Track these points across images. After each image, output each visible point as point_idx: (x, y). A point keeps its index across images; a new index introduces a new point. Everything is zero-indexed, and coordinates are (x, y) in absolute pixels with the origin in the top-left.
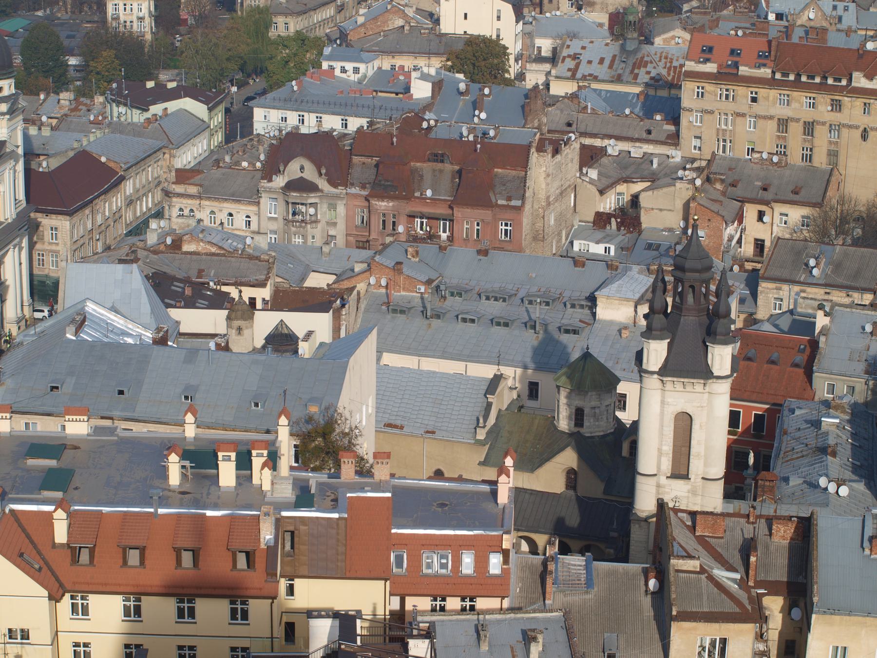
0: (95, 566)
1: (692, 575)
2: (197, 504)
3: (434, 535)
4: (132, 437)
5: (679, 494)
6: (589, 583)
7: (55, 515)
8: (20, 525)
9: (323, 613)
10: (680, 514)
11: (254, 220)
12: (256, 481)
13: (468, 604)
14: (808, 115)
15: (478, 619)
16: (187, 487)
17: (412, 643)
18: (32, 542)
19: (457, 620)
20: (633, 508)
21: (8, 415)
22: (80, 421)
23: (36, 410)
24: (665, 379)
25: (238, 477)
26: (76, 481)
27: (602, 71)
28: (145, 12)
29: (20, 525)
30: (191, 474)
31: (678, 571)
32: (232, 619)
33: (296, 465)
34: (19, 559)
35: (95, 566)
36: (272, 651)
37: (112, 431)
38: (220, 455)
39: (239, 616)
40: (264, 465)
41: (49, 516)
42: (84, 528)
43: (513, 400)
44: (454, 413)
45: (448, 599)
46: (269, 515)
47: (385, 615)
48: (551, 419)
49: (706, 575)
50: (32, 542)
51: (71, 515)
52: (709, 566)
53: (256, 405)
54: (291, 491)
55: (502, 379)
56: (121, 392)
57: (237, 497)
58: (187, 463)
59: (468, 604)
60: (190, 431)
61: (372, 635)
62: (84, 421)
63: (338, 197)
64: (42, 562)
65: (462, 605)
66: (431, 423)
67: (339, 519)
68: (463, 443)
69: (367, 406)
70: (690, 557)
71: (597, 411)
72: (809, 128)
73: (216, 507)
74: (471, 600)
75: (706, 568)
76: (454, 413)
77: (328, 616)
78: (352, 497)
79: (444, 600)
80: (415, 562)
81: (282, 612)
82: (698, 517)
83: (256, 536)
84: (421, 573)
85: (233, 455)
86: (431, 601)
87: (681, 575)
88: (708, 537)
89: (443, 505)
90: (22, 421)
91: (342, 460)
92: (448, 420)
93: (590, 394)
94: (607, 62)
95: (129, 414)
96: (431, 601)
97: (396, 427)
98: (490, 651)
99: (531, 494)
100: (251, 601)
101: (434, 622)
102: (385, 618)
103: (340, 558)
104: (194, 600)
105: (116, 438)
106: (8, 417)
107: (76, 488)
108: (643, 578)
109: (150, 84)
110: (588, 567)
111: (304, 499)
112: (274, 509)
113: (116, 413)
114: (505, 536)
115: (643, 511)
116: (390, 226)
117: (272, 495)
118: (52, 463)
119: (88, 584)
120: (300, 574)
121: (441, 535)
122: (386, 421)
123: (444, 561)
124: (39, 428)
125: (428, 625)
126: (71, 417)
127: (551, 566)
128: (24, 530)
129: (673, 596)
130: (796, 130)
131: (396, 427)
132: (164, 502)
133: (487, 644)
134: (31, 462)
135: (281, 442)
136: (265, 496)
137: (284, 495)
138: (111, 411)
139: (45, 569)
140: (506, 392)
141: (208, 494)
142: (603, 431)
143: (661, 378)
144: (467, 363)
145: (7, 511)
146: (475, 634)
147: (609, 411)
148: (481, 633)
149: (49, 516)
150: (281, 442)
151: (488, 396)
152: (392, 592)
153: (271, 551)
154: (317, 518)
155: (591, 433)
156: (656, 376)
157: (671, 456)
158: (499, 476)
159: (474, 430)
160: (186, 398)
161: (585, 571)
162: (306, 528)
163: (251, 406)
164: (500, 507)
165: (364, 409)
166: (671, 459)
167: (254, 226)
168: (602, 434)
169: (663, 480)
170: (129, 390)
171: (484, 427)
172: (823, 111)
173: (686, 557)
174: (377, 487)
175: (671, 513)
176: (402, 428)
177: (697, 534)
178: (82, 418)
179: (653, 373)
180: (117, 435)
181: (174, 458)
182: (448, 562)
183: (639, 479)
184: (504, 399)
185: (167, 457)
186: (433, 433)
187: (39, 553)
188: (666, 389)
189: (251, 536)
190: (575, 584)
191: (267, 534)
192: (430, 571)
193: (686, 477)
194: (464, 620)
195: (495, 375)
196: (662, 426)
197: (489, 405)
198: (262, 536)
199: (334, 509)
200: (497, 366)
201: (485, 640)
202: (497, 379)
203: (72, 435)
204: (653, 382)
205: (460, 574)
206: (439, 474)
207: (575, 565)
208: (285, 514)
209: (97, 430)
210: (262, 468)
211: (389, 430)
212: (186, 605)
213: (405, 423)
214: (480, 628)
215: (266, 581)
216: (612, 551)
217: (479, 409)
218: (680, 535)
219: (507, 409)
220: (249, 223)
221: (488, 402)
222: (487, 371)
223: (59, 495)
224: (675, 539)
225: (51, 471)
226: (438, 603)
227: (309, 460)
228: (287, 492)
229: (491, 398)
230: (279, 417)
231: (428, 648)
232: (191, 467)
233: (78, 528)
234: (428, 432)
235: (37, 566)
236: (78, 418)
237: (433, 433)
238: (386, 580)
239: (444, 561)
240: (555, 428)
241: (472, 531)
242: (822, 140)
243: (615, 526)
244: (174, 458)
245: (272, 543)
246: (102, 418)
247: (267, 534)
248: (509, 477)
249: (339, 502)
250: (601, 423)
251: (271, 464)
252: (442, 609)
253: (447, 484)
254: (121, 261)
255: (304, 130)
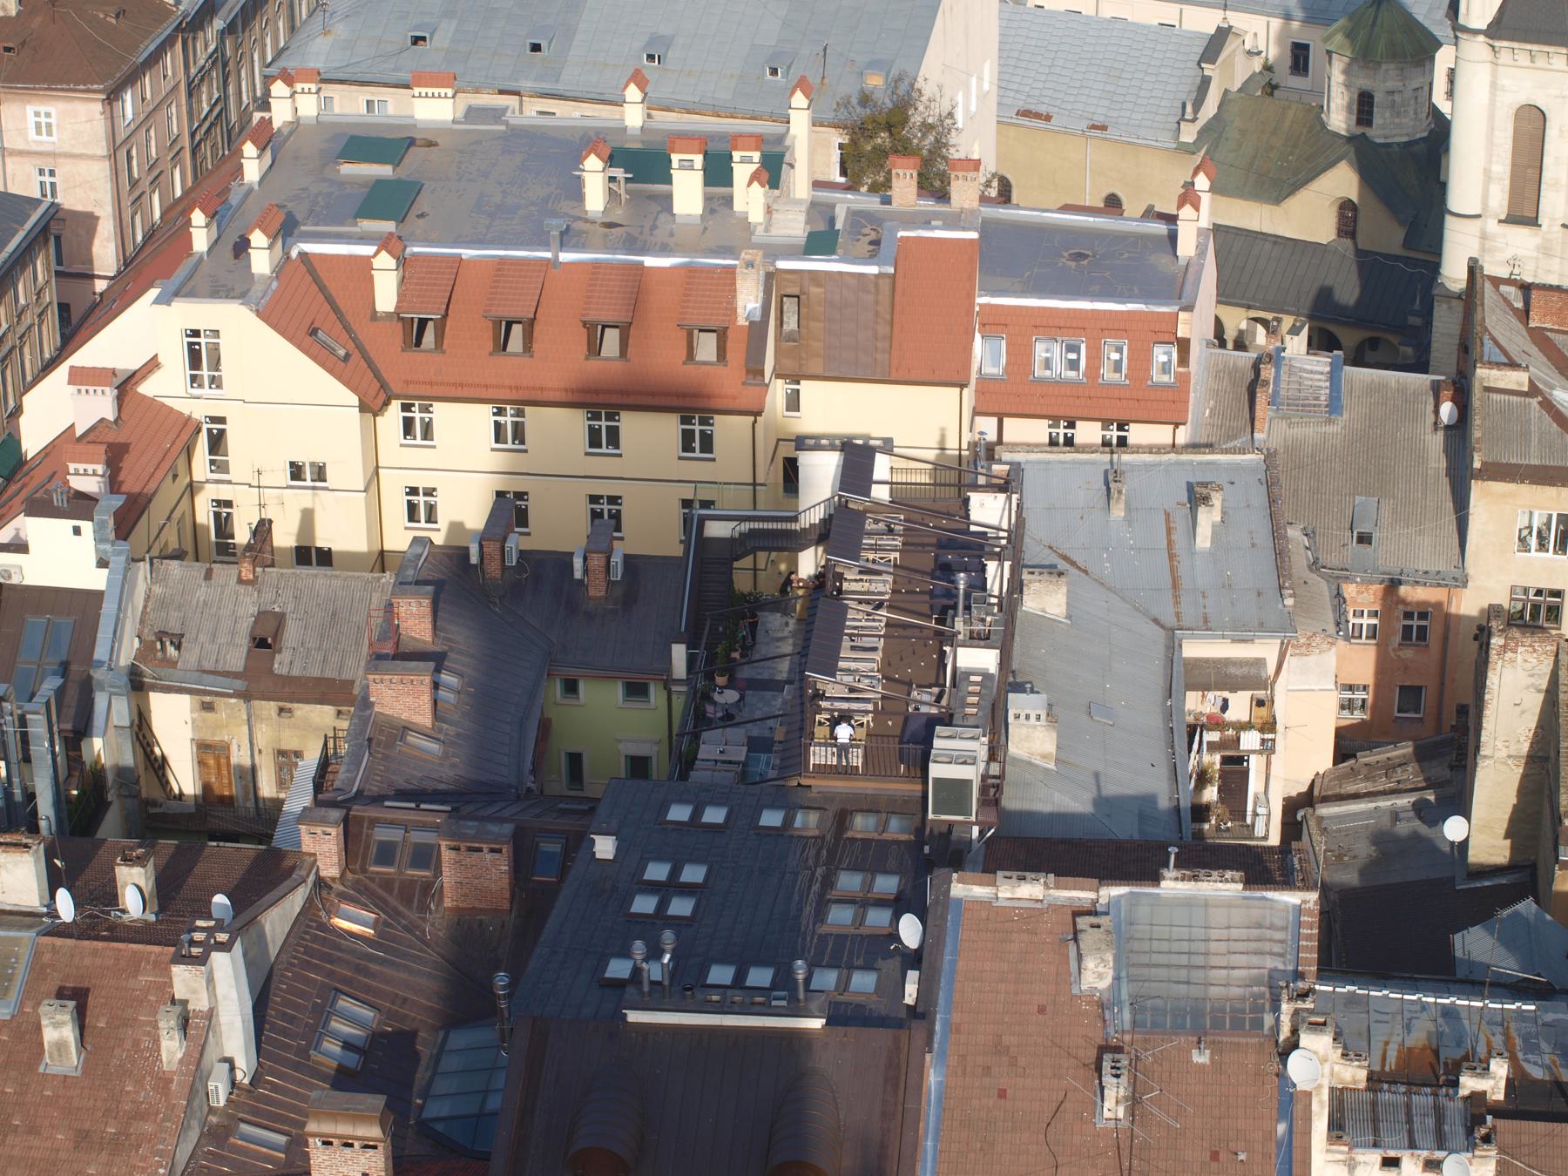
0: (444, 352)
1: (1514, 399)
2: (635, 244)
3: (1057, 309)
4: (533, 126)
5: (1520, 253)
6: (1334, 406)
7: (376, 263)
8: (316, 280)
9: (824, 442)
10: (1503, 288)
12: (738, 206)
13: (1114, 434)
15: (1111, 462)
16: (618, 215)
17: (975, 498)
18: (336, 310)
19: (1074, 462)
20: (1440, 274)
21: (313, 87)
22: (440, 97)
23: (385, 79)
24: (1497, 44)
25: (708, 199)
26: (424, 203)
29: (316, 280)
30: (627, 192)
31: (1488, 389)
32: (684, 450)
33: (842, 180)
34: (309, 339)
35: (444, 352)
36: (755, 509)
37: (497, 114)
38: (675, 158)
39: (697, 445)
40: (755, 177)
41: (365, 264)
42: (428, 285)
43: (1254, 74)
44: (1142, 93)
45: (1078, 423)
46: (753, 266)
47: (960, 449)
48: (1317, 110)
49: (1540, 399)
50: (336, 310)
51: (403, 262)
52: (1546, 384)
53: (774, 72)
54: (802, 225)
55: (1231, 37)
56: (536, 48)
57: (703, 233)
58: (619, 173)
59: (1114, 434)
60: (633, 116)
61: (941, 485)
62: (446, 97)
64: (351, 345)
65: (1104, 436)
66: (1100, 111)
67: (880, 276)
68: (1156, 148)
69: (980, 79)
70: (1513, 365)
71: (1397, 98)
73: (665, 250)
74: (1121, 427)
75: (1541, 386)
76: (1142, 93)
77: (832, 448)
78: (908, 238)
79: (1071, 425)
80: (1020, 357)
81: (779, 440)
82: (1534, 294)
83: (728, 303)
84: (1031, 377)
85: (698, 160)
86: (1050, 426)
87: (1494, 396)
88: (1551, 330)
89: (1080, 256)
90: (361, 98)
91: (894, 172)
92: (1131, 106)
93: (1384, 66)
95: (547, 86)
96: (1050, 426)
97: (1038, 116)
98: (1128, 521)
99: (1275, 243)
100: (718, 419)
101: (1019, 464)
102: (960, 455)
103: (879, 345)
104: (618, 414)
105: (503, 128)
106: (314, 90)
107: (421, 216)
108: (1431, 400)
110: (1334, 377)
111: (821, 241)
112: (766, 256)
113: (525, 84)
114: (1182, 315)
115: (1455, 281)
117: (767, 230)
118: (385, 171)
119: (431, 384)
120: (811, 372)
121: (1069, 310)
122: (1021, 105)
123: (1073, 356)
124: (391, 110)
125: (1007, 467)
126: (423, 91)
127: (1268, 372)
128: (322, 289)
129: (1477, 434)
131: (1038, 116)
132: (567, 239)
133: (1122, 505)
134: (348, 169)
135: (795, 137)
136: (752, 233)
137: (790, 232)
138: (517, 80)
139: (356, 356)
140: (1240, 59)
141: (654, 227)
142: (1407, 135)
143: (1491, 42)
144: (1184, 6)
145: (294, 254)
146: (1105, 488)
147: (1419, 100)
148: (1112, 485)
149: (365, 264)
150: (795, 137)
151: (1203, 65)
152: (978, 410)
153: (757, 331)
154: (840, 273)
155: (1386, 137)
156: (1481, 38)
157: (1507, 182)
158: (1180, 207)
159: (1176, 125)
160: (651, 57)
161: (1328, 384)
162: (822, 290)
163: (764, 74)
164: (1182, 262)
165: (974, 81)
166: (1507, 188)
168: (1405, 139)
169: (1492, 226)
170: (550, 43)
171: (1194, 120)
173: (1505, 364)
174: (953, 222)
175: (1488, 285)
176: (1048, 118)
177: (1532, 324)
178: (443, 91)
179: (1476, 32)
180: (507, 123)
181: (593, 163)
182: (1079, 359)
183: (1450, 222)
184: (1232, 73)
185: (580, 159)
186: (1104, 128)
187: (347, 328)
188: (1500, 61)
189: (720, 303)
190: (1309, 405)
191: (748, 300)
192: (1048, 373)
193: (1533, 222)
194: (1086, 463)
195: (1219, 29)
196: (1491, 128)
197: (1206, 81)
198: (740, 304)
199: (872, 258)
200: (1222, 12)
201: (1119, 498)
202: (1222, 35)
203: (426, 122)
204: (1477, 47)
205: (1100, 381)
206: (1113, 204)
207: (1311, 372)
208: (783, 265)
209: (472, 114)
210: (749, 184)
211: (1025, 121)
212: (604, 424)
213: (1052, 110)
214: (1111, 478)
215: (744, 383)
216: (1409, 350)
217: (1186, 90)
218: (1497, 323)
219: (1240, 90)
221: (1203, 76)
222: (1205, 21)
223: (389, 226)
224: (1486, 330)
225: (380, 184)
226: (1062, 431)
227: (862, 171)
228: (794, 226)
229: (1208, 69)
230: (793, 93)
231: (1004, 509)
232: (627, 179)
233: (417, 284)
234: (1094, 127)
235: (342, 352)
236: (436, 91)
237: (1104, 128)
238: (962, 386)
239: (1073, 356)
240: (1323, 125)
241: (1125, 303)
243: (1417, 306)
244: (593, 163)
245: (757, 318)
246: (501, 92)
247: (748, 300)
248: (1197, 209)
249: (882, 246)
250: (1405, 121)
251: (765, 176)
252: (1069, 442)
253: (1091, 219)
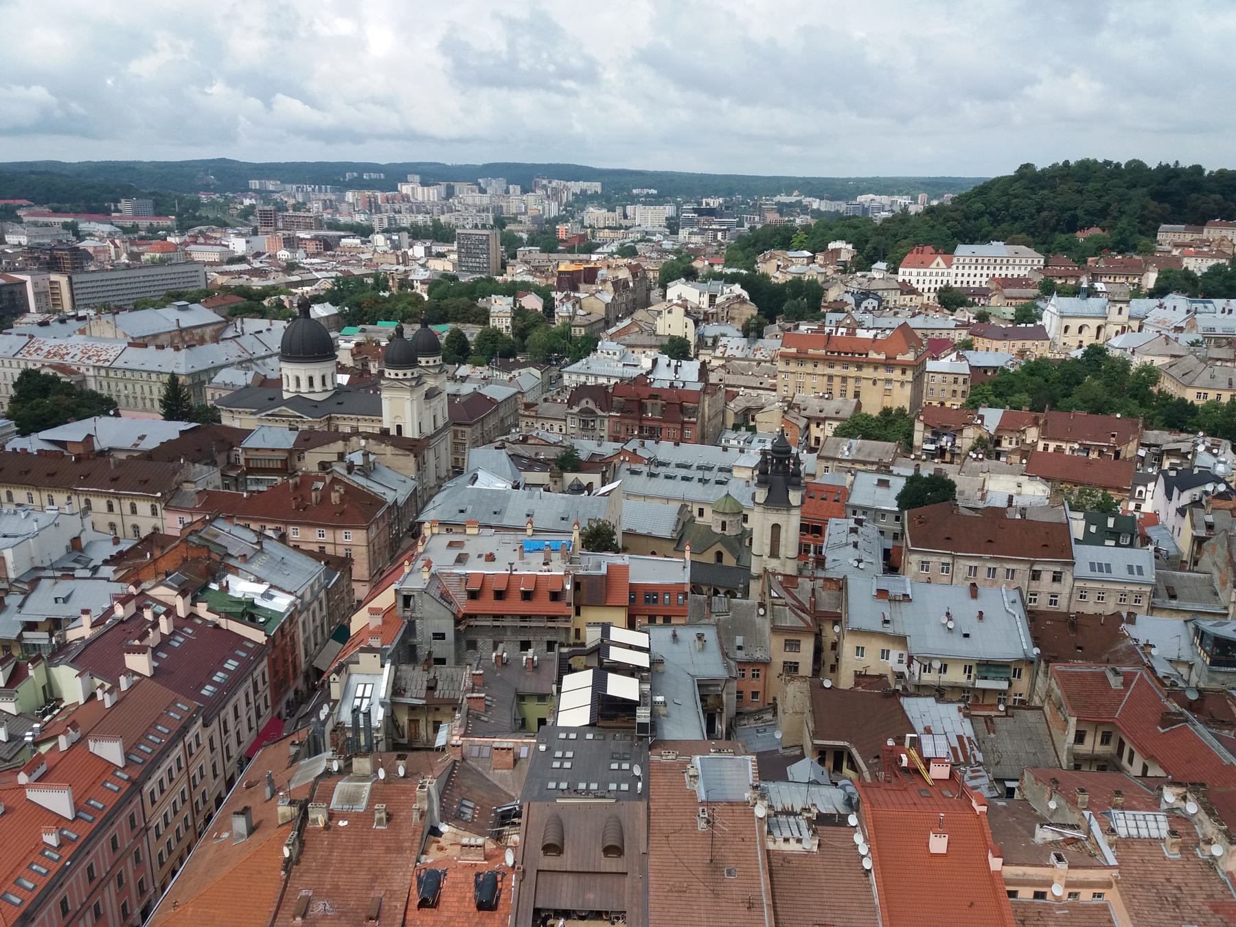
11: (564, 428)
14: (845, 372)
27: (738, 354)
28: (508, 324)
63: (605, 417)
72: (844, 379)
94: (740, 349)
109: (511, 360)
116: (630, 431)
130: (837, 381)
167: (564, 431)
172: (852, 371)
220: (561, 430)
242: (851, 386)
254: (496, 448)
255: (588, 384)
